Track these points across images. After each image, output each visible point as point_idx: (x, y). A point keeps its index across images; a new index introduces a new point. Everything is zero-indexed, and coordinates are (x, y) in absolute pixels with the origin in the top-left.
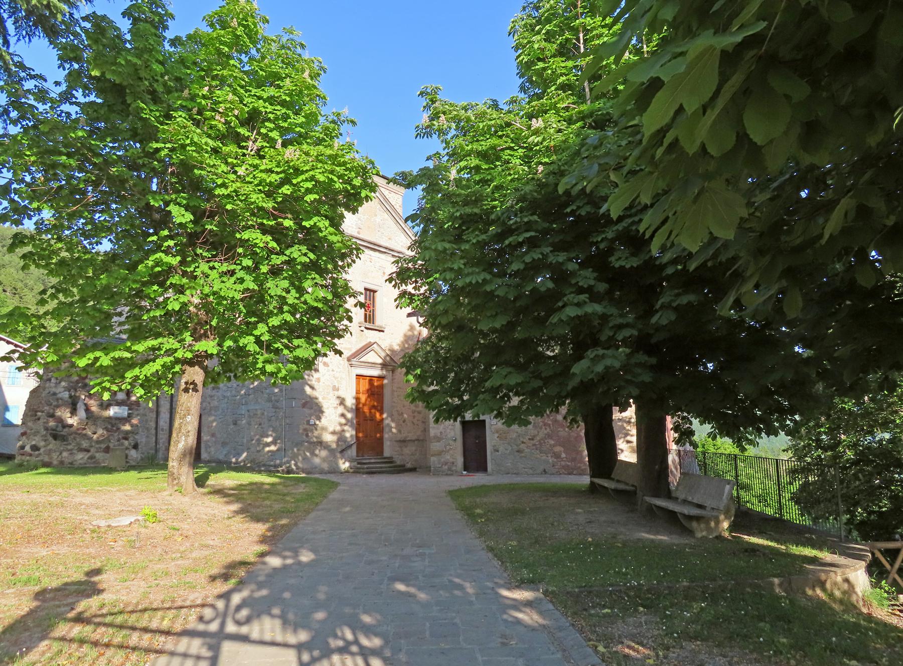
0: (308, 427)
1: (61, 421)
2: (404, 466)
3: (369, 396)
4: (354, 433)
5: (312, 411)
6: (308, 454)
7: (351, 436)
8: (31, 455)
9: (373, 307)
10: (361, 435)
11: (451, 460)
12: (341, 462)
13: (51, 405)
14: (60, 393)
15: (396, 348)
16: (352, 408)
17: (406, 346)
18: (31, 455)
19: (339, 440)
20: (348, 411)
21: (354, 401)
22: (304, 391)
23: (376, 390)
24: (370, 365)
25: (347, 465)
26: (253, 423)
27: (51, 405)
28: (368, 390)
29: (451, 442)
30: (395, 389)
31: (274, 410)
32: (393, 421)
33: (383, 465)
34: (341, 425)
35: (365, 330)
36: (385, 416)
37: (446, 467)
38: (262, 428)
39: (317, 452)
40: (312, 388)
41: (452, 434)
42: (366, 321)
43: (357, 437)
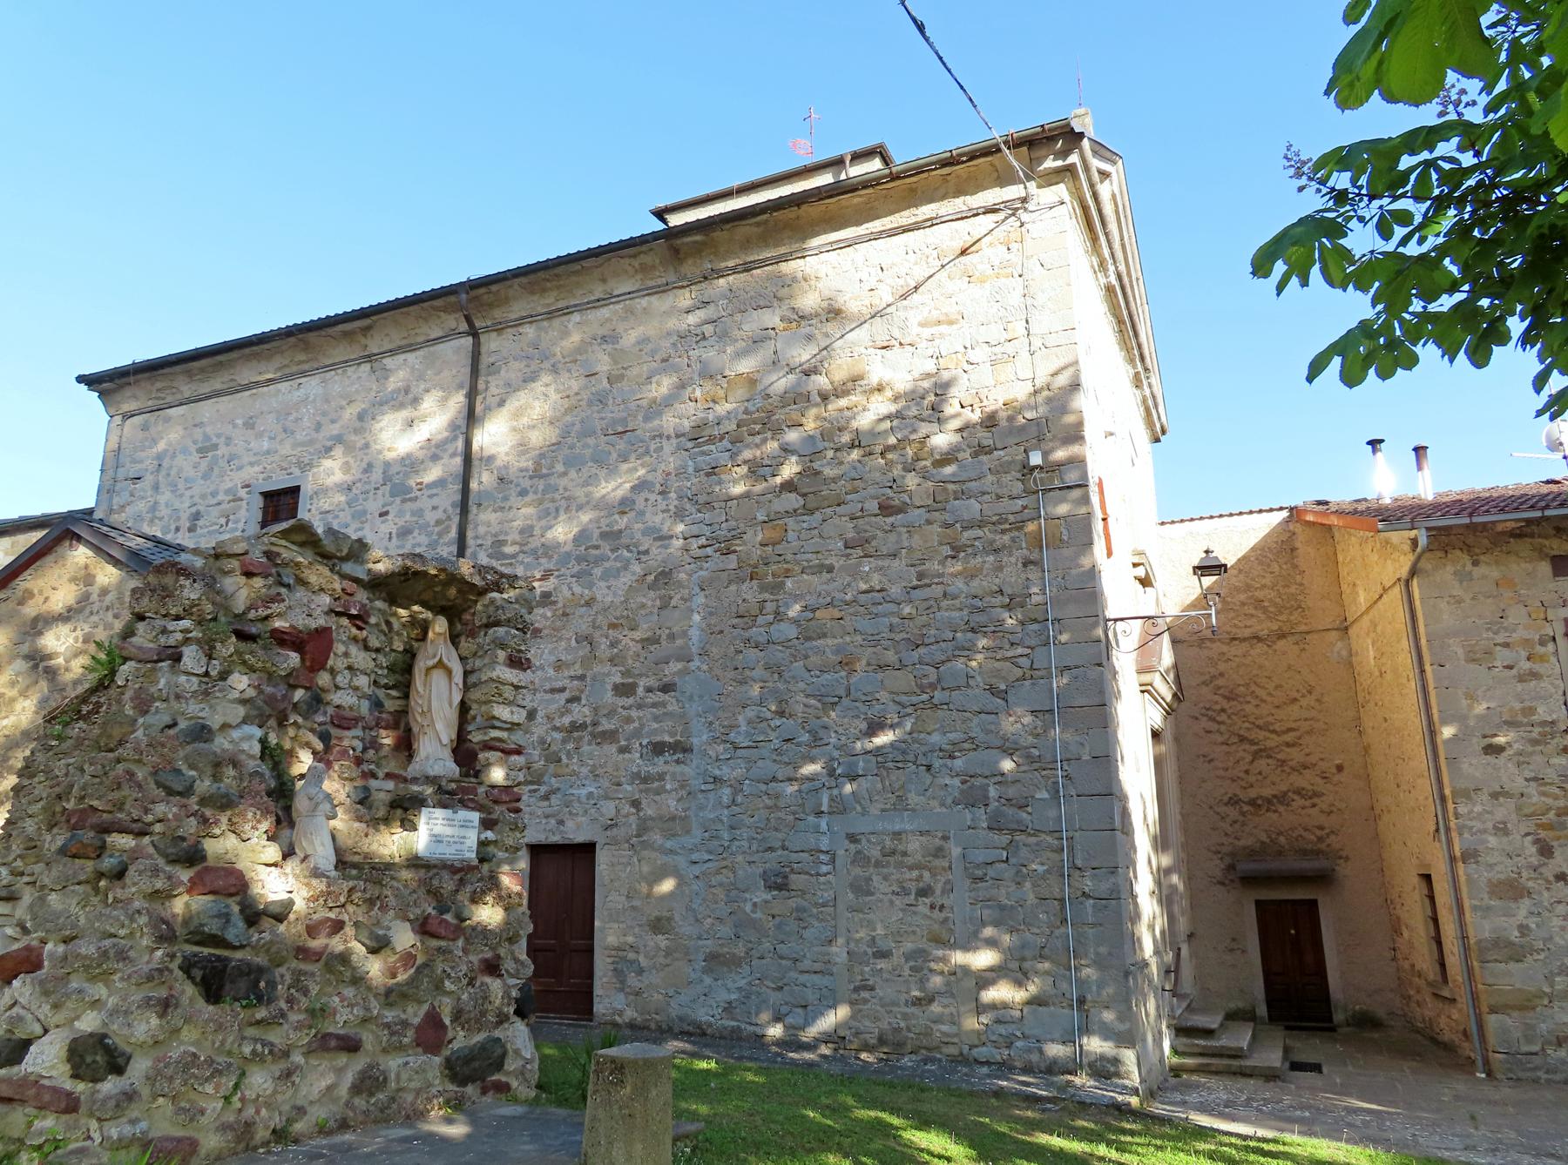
1: (234, 885)
8: (70, 1105)
13: (188, 791)
14: (225, 726)
18: (70, 1105)
27: (188, 791)
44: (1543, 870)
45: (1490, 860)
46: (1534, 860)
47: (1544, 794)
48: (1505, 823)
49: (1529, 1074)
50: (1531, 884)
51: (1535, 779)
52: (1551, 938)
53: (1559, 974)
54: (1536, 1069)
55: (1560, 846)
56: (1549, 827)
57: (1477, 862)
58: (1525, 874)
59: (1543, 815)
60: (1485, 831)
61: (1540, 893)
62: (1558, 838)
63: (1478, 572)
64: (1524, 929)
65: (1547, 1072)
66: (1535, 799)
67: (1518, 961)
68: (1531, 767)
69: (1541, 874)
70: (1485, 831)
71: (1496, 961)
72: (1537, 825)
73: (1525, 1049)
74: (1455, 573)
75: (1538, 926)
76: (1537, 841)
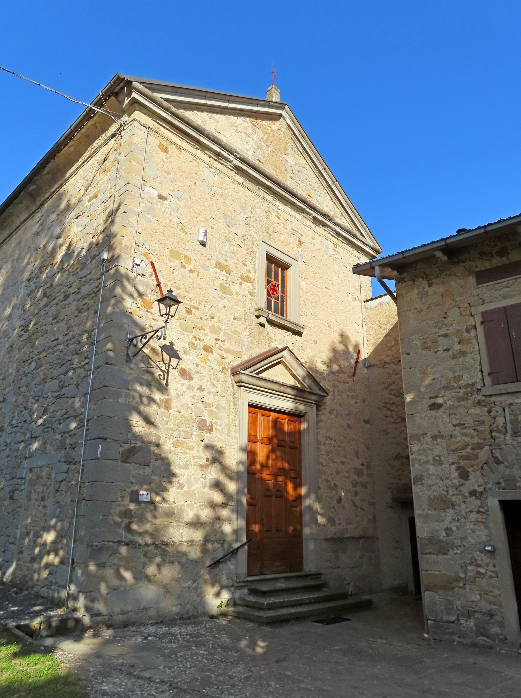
0: (132, 506)
2: (344, 596)
3: (273, 451)
4: (241, 523)
5: (148, 471)
6: (128, 575)
7: (236, 532)
9: (283, 291)
10: (256, 528)
11: (485, 606)
12: (210, 592)
15: (322, 367)
16: (238, 473)
17: (335, 367)
19: (207, 539)
20: (231, 478)
21: (244, 457)
22: (128, 426)
23: (287, 438)
24: (276, 387)
25: (225, 596)
26: (33, 496)
28: (270, 440)
29: (480, 557)
30: (322, 439)
31: (65, 467)
32: (319, 499)
33: (306, 597)
34: (213, 506)
35: (266, 324)
36: (303, 491)
37: (471, 623)
38: (44, 507)
39: (151, 570)
40: (149, 421)
41: (482, 534)
42: (269, 307)
43: (249, 532)
44: (462, 488)
45: (430, 482)
46: (456, 482)
47: (464, 435)
48: (439, 456)
49: (447, 637)
50: (454, 499)
51: (459, 425)
52: (465, 538)
53: (470, 564)
54: (452, 634)
55: (473, 471)
56: (467, 458)
57: (422, 484)
58: (450, 492)
59: (463, 449)
60: (427, 462)
61: (459, 505)
62: (473, 466)
63: (431, 290)
64: (448, 531)
65: (459, 637)
66: (459, 439)
67: (444, 554)
68: (457, 417)
69: (460, 491)
70: (427, 462)
71: (430, 553)
72: (459, 457)
73: (445, 618)
74: (418, 294)
75: (457, 528)
76: (458, 469)
